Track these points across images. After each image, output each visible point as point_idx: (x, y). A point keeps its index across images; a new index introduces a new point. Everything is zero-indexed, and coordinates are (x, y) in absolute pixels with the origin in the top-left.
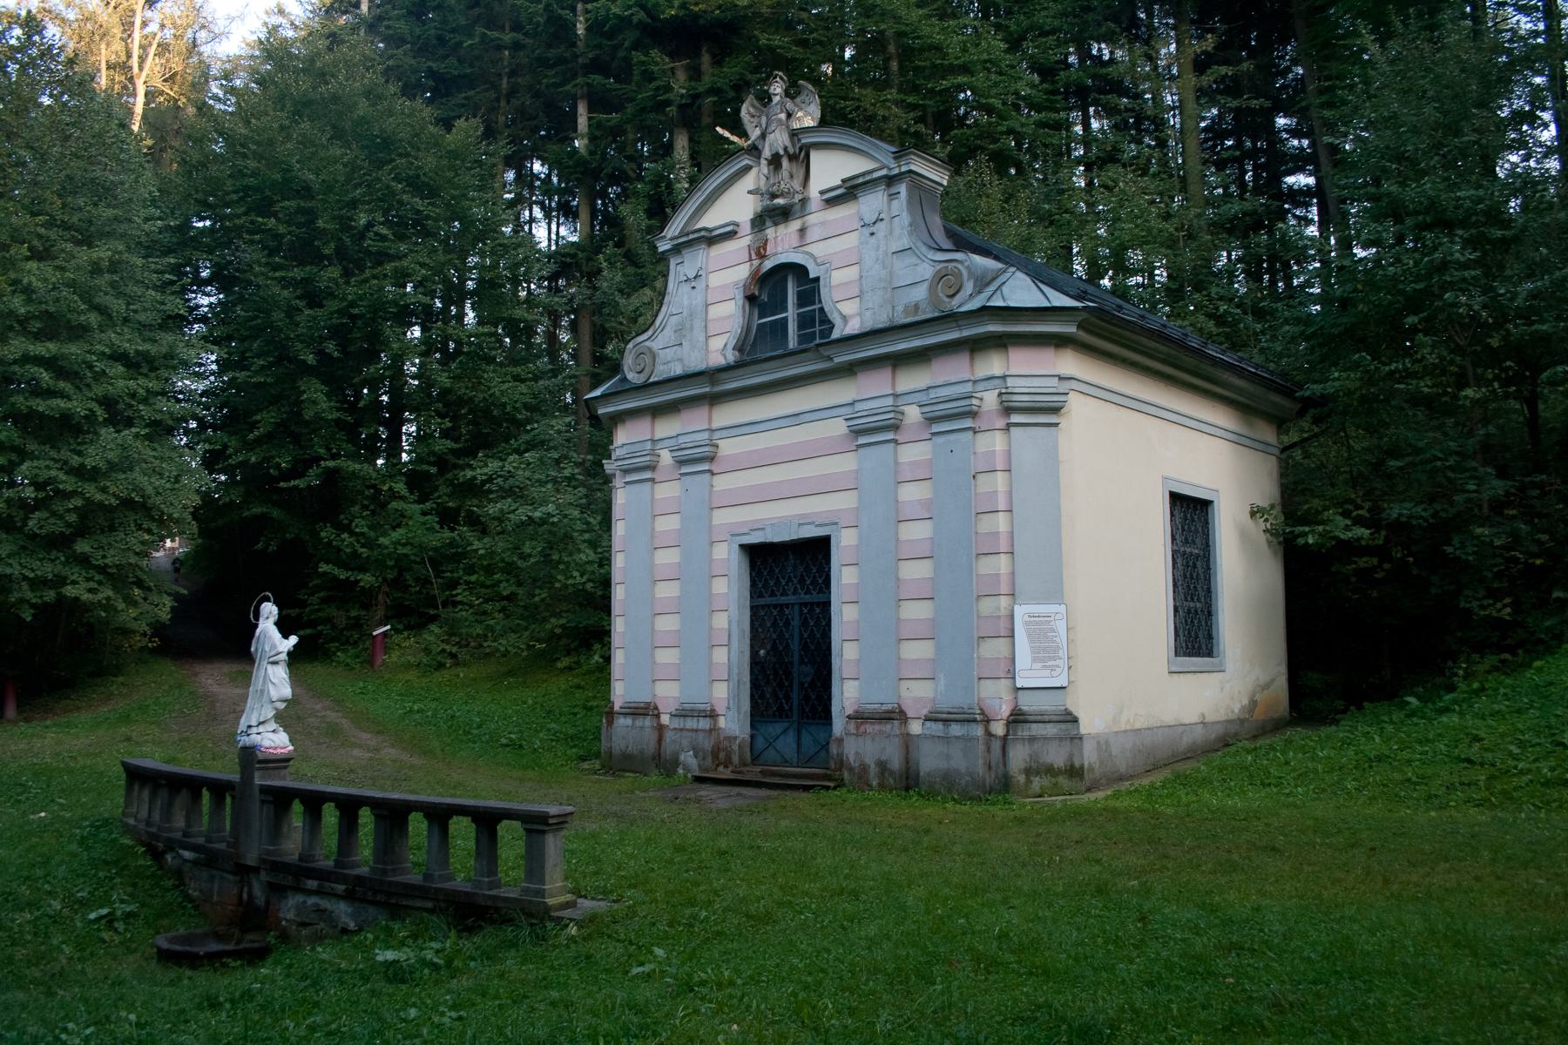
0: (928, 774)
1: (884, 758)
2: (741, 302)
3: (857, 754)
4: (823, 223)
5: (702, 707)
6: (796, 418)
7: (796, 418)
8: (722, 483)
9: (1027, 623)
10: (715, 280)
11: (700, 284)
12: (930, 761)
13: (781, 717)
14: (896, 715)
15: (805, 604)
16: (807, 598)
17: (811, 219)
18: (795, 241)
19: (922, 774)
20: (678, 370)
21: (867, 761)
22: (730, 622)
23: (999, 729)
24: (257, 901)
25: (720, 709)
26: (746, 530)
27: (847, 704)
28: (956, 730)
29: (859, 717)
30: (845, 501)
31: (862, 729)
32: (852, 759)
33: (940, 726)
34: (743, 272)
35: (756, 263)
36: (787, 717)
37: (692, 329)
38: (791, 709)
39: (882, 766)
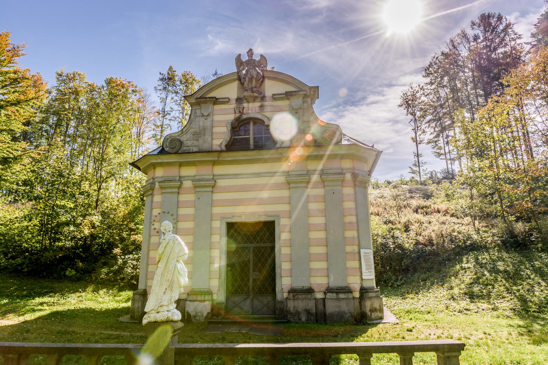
0: (331, 314)
1: (308, 308)
2: (229, 128)
3: (294, 307)
4: (272, 106)
5: (206, 290)
6: (258, 175)
7: (258, 175)
8: (217, 196)
9: (364, 256)
10: (217, 118)
11: (210, 119)
12: (331, 307)
14: (310, 291)
17: (266, 103)
18: (258, 110)
19: (327, 314)
20: (195, 149)
21: (300, 310)
22: (220, 253)
23: (357, 295)
25: (215, 290)
26: (231, 216)
27: (284, 287)
28: (342, 296)
29: (293, 291)
30: (285, 207)
31: (296, 297)
33: (335, 295)
34: (231, 117)
35: (238, 115)
37: (204, 134)
39: (308, 312)
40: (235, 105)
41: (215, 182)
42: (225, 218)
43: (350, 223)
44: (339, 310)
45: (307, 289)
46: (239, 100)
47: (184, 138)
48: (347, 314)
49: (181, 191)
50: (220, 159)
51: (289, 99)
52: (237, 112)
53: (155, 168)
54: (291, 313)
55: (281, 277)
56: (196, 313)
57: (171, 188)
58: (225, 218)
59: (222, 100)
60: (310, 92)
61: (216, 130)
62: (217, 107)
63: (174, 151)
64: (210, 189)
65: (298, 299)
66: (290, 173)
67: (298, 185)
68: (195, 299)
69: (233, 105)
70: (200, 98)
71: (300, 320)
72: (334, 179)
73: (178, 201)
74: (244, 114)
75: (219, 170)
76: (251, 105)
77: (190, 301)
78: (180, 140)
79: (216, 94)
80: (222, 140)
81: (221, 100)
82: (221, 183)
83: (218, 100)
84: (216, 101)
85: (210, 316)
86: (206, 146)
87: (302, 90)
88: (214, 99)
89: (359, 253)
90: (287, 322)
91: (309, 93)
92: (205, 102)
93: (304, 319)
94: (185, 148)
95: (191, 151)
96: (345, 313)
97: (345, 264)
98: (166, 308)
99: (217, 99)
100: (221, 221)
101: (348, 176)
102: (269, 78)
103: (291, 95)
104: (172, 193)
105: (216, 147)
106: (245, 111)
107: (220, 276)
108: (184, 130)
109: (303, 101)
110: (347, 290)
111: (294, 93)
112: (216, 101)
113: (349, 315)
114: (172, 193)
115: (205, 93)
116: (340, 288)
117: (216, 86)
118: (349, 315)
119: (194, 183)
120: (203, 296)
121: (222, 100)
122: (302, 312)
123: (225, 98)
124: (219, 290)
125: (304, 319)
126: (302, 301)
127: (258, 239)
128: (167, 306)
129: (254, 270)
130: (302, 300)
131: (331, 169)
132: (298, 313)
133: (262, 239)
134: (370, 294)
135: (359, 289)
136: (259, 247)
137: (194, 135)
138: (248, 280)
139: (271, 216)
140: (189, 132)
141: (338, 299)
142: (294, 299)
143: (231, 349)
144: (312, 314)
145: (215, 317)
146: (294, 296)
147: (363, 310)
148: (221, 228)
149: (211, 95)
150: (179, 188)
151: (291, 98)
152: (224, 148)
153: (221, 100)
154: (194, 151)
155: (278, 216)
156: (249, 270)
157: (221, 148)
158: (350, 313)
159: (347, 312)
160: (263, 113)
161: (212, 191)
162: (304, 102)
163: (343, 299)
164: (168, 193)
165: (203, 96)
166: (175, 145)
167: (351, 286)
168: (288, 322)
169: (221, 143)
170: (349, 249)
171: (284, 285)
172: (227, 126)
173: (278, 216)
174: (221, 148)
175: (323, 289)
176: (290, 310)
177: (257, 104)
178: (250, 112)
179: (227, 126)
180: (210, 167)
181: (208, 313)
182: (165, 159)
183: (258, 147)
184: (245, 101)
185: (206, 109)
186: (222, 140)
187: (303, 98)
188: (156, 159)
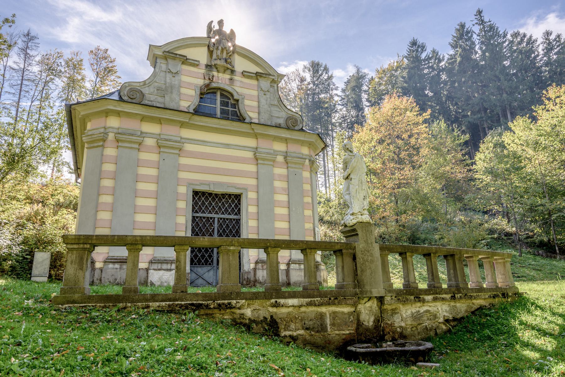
4: (241, 82)
6: (227, 146)
7: (227, 146)
8: (183, 161)
10: (184, 78)
11: (177, 78)
13: (206, 264)
15: (221, 219)
16: (223, 216)
17: (235, 78)
18: (228, 82)
22: (186, 221)
24: (366, 323)
26: (198, 183)
27: (251, 258)
32: (261, 279)
33: (297, 265)
34: (201, 82)
35: (207, 82)
36: (210, 264)
37: (172, 92)
38: (212, 261)
47: (146, 91)
50: (191, 122)
52: (207, 78)
54: (260, 283)
56: (162, 282)
57: (131, 142)
58: (193, 184)
59: (193, 62)
60: (278, 79)
62: (185, 67)
64: (177, 152)
67: (266, 162)
68: (159, 267)
72: (297, 162)
75: (186, 133)
76: (221, 75)
77: (154, 269)
80: (191, 103)
88: (185, 58)
92: (174, 59)
104: (131, 148)
106: (214, 80)
114: (131, 148)
117: (187, 45)
120: (169, 265)
121: (193, 62)
123: (196, 61)
131: (294, 152)
133: (226, 210)
139: (238, 188)
140: (152, 86)
142: (263, 269)
146: (262, 267)
151: (260, 79)
152: (192, 111)
153: (190, 61)
160: (233, 87)
165: (171, 51)
169: (189, 106)
173: (246, 190)
176: (259, 280)
178: (220, 81)
188: (115, 106)
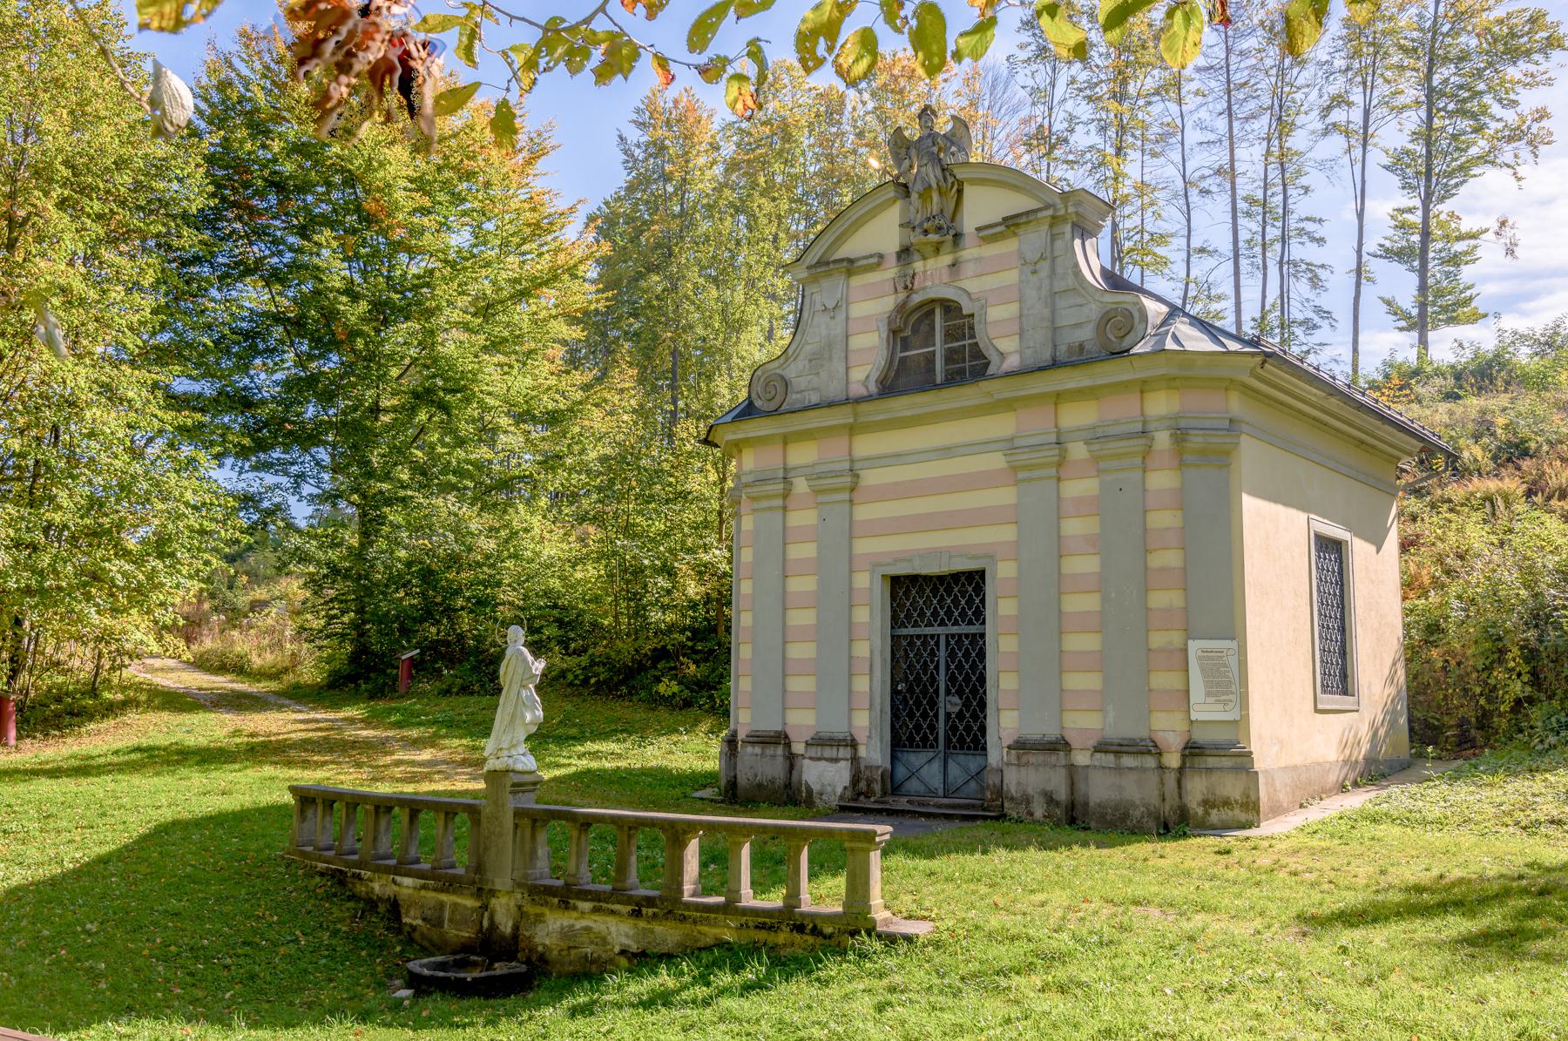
0: (1099, 805)
1: (1048, 788)
2: (884, 335)
3: (1019, 784)
4: (978, 260)
5: (841, 736)
6: (946, 452)
7: (946, 452)
8: (863, 512)
9: (1200, 658)
11: (841, 316)
12: (1100, 790)
13: (925, 747)
14: (1059, 746)
15: (953, 636)
16: (955, 630)
19: (1092, 804)
20: (814, 398)
21: (1030, 791)
22: (872, 651)
23: (1173, 760)
24: (502, 928)
25: (861, 737)
27: (1004, 734)
28: (1128, 761)
29: (1021, 746)
30: (1007, 533)
31: (1024, 759)
32: (1013, 791)
33: (1111, 757)
34: (888, 303)
35: (902, 296)
36: (932, 746)
37: (830, 358)
38: (936, 739)
39: (1050, 799)
40: (895, 270)
41: (858, 476)
42: (882, 565)
43: (1163, 570)
44: (1118, 797)
45: (1050, 743)
46: (905, 253)
47: (790, 373)
48: (1137, 807)
49: (791, 503)
50: (861, 420)
51: (1015, 234)
52: (900, 289)
53: (740, 451)
54: (1012, 799)
55: (998, 710)
56: (823, 785)
57: (768, 497)
58: (882, 565)
59: (865, 262)
60: (1066, 207)
61: (857, 342)
62: (856, 281)
63: (772, 406)
64: (846, 496)
65: (1027, 764)
66: (1018, 443)
67: (1036, 474)
68: (819, 755)
69: (890, 271)
70: (819, 263)
71: (1032, 815)
72: (1121, 451)
73: (784, 527)
74: (916, 293)
75: (865, 445)
76: (931, 263)
77: (811, 758)
78: (782, 377)
79: (851, 248)
80: (870, 367)
81: (861, 263)
82: (872, 478)
83: (856, 264)
84: (851, 266)
85: (849, 794)
86: (834, 390)
87: (1048, 207)
88: (845, 264)
89: (1185, 651)
90: (997, 818)
91: (1062, 212)
92: (829, 274)
93: (1039, 812)
94: (794, 396)
95: (807, 404)
96: (1133, 804)
97: (1148, 683)
98: (506, 752)
99: (851, 261)
100: (873, 572)
101: (1163, 439)
102: (974, 182)
103: (1017, 225)
104: (770, 508)
105: (857, 390)
106: (916, 286)
107: (871, 705)
108: (790, 351)
109: (1052, 235)
110: (1152, 748)
111: (1024, 219)
112: (851, 266)
113: (1142, 809)
114: (770, 508)
115: (825, 253)
116: (1125, 742)
117: (853, 224)
118: (1142, 809)
119: (812, 483)
120: (835, 749)
122: (1036, 796)
123: (871, 256)
124: (869, 737)
125: (1039, 812)
126: (1037, 770)
127: (956, 614)
128: (509, 749)
129: (948, 693)
130: (1037, 766)
131: (1116, 422)
132: (1027, 800)
133: (963, 614)
134: (1210, 759)
135: (1182, 746)
136: (960, 636)
137: (810, 361)
138: (936, 715)
139: (974, 557)
140: (801, 357)
141: (1119, 769)
142: (1019, 765)
143: (569, 812)
144: (1057, 804)
145: (862, 798)
146: (1018, 758)
147: (1185, 800)
148: (871, 590)
149: (839, 254)
150: (785, 496)
151: (1021, 231)
152: (873, 389)
153: (861, 263)
154: (813, 402)
155: (992, 557)
156: (937, 692)
157: (867, 387)
158: (1146, 806)
159: (1137, 802)
160: (958, 284)
161: (851, 501)
162: (1053, 238)
163: (1131, 769)
164: (765, 509)
165: (824, 259)
166: (773, 392)
167: (1159, 737)
168: (1002, 817)
169: (868, 377)
170: (1158, 639)
171: (1005, 729)
172: (878, 330)
173: (992, 557)
174: (867, 387)
175: (1092, 743)
176: (1009, 791)
177: (946, 259)
178: (929, 283)
179: (878, 330)
180: (844, 441)
181: (845, 788)
182: (754, 428)
183: (956, 378)
184: (916, 256)
185: (826, 292)
186: (869, 367)
187: (1051, 226)
188: (734, 433)
